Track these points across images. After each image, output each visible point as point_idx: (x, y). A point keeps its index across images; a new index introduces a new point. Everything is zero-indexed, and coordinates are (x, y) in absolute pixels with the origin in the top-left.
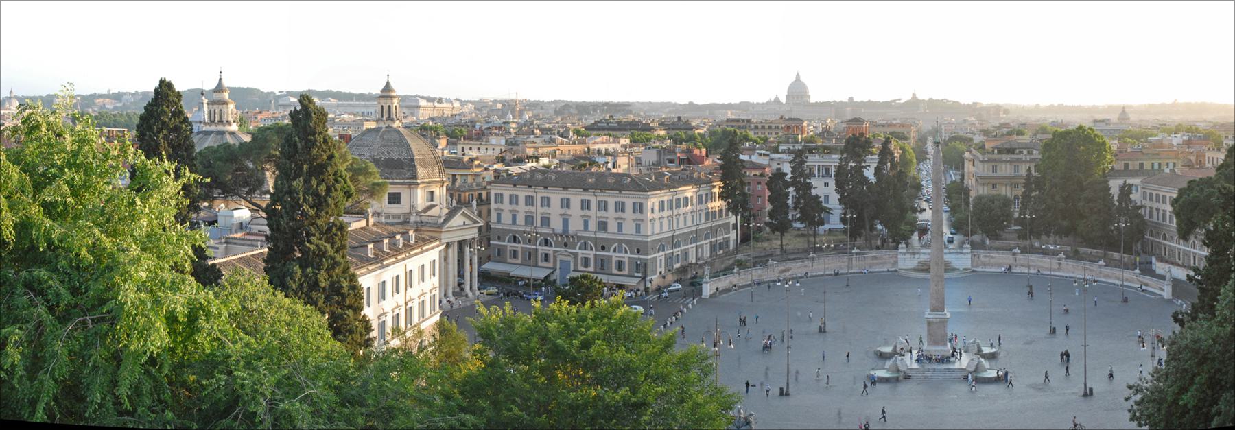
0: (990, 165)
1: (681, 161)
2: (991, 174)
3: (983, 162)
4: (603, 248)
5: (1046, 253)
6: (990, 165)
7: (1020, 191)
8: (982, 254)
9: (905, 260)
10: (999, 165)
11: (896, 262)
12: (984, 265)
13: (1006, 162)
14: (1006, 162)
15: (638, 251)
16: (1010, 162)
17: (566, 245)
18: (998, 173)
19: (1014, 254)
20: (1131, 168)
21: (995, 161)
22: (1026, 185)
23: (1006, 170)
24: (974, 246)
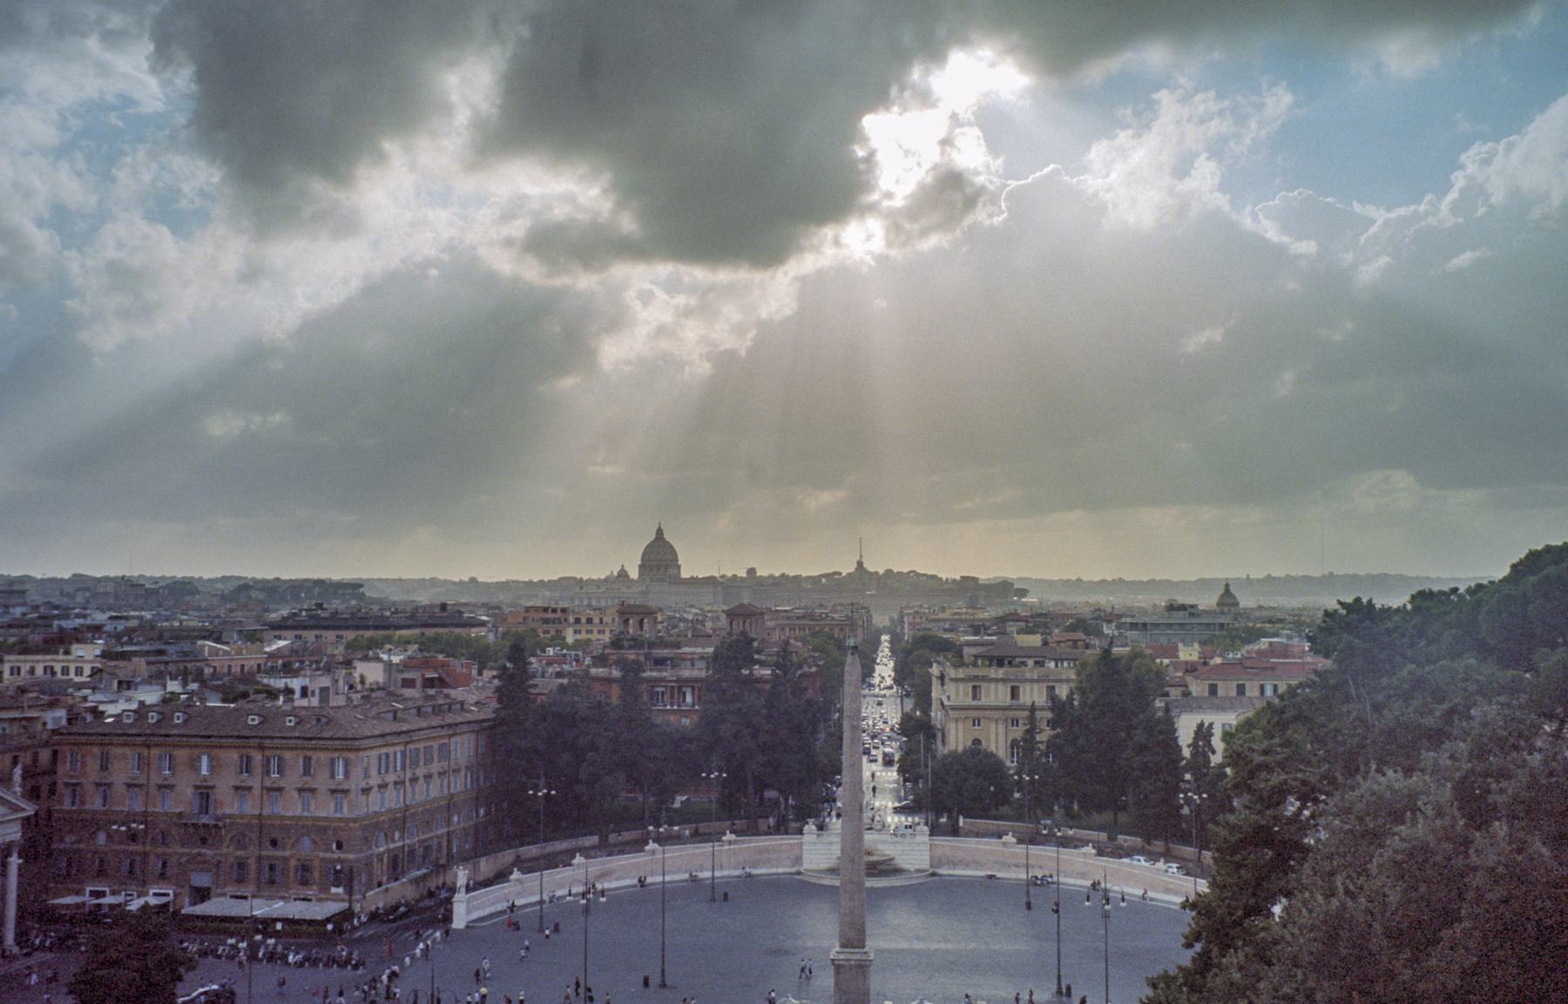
0: (970, 685)
1: (429, 683)
2: (969, 701)
3: (956, 680)
4: (274, 843)
5: (1065, 843)
6: (970, 685)
7: (1018, 732)
8: (946, 843)
9: (817, 850)
10: (984, 685)
11: (798, 860)
12: (953, 863)
13: (997, 680)
14: (997, 680)
15: (340, 846)
16: (1004, 681)
17: (204, 841)
18: (984, 701)
19: (1004, 844)
20: (1220, 692)
21: (976, 678)
22: (1032, 719)
23: (996, 695)
24: (935, 830)
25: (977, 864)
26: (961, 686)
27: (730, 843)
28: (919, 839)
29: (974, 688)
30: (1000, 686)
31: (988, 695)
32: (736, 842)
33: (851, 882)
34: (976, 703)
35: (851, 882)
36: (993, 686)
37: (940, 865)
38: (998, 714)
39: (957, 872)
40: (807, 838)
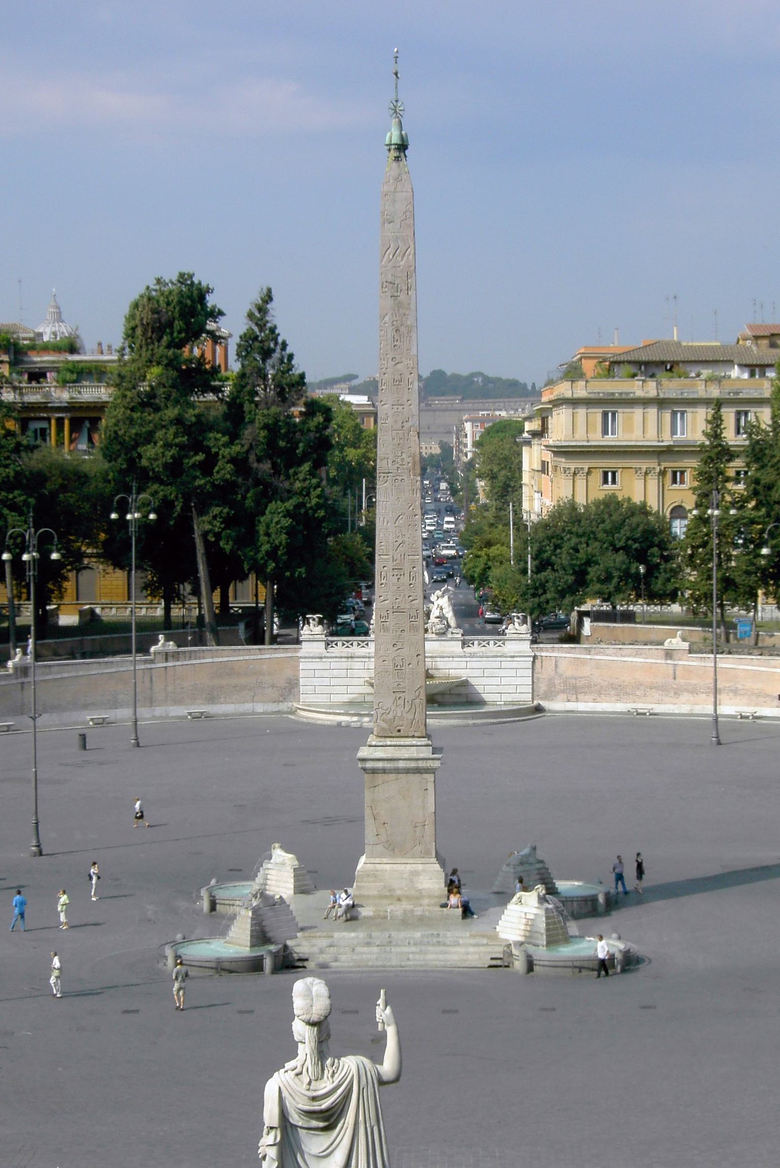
2: (597, 439)
9: (325, 675)
12: (574, 690)
13: (645, 402)
14: (645, 402)
19: (669, 654)
25: (620, 690)
26: (581, 412)
27: (167, 656)
28: (510, 647)
29: (605, 415)
30: (652, 412)
31: (629, 428)
32: (176, 656)
33: (398, 611)
34: (610, 440)
35: (398, 611)
36: (638, 412)
37: (550, 695)
38: (644, 464)
39: (581, 706)
40: (306, 648)
